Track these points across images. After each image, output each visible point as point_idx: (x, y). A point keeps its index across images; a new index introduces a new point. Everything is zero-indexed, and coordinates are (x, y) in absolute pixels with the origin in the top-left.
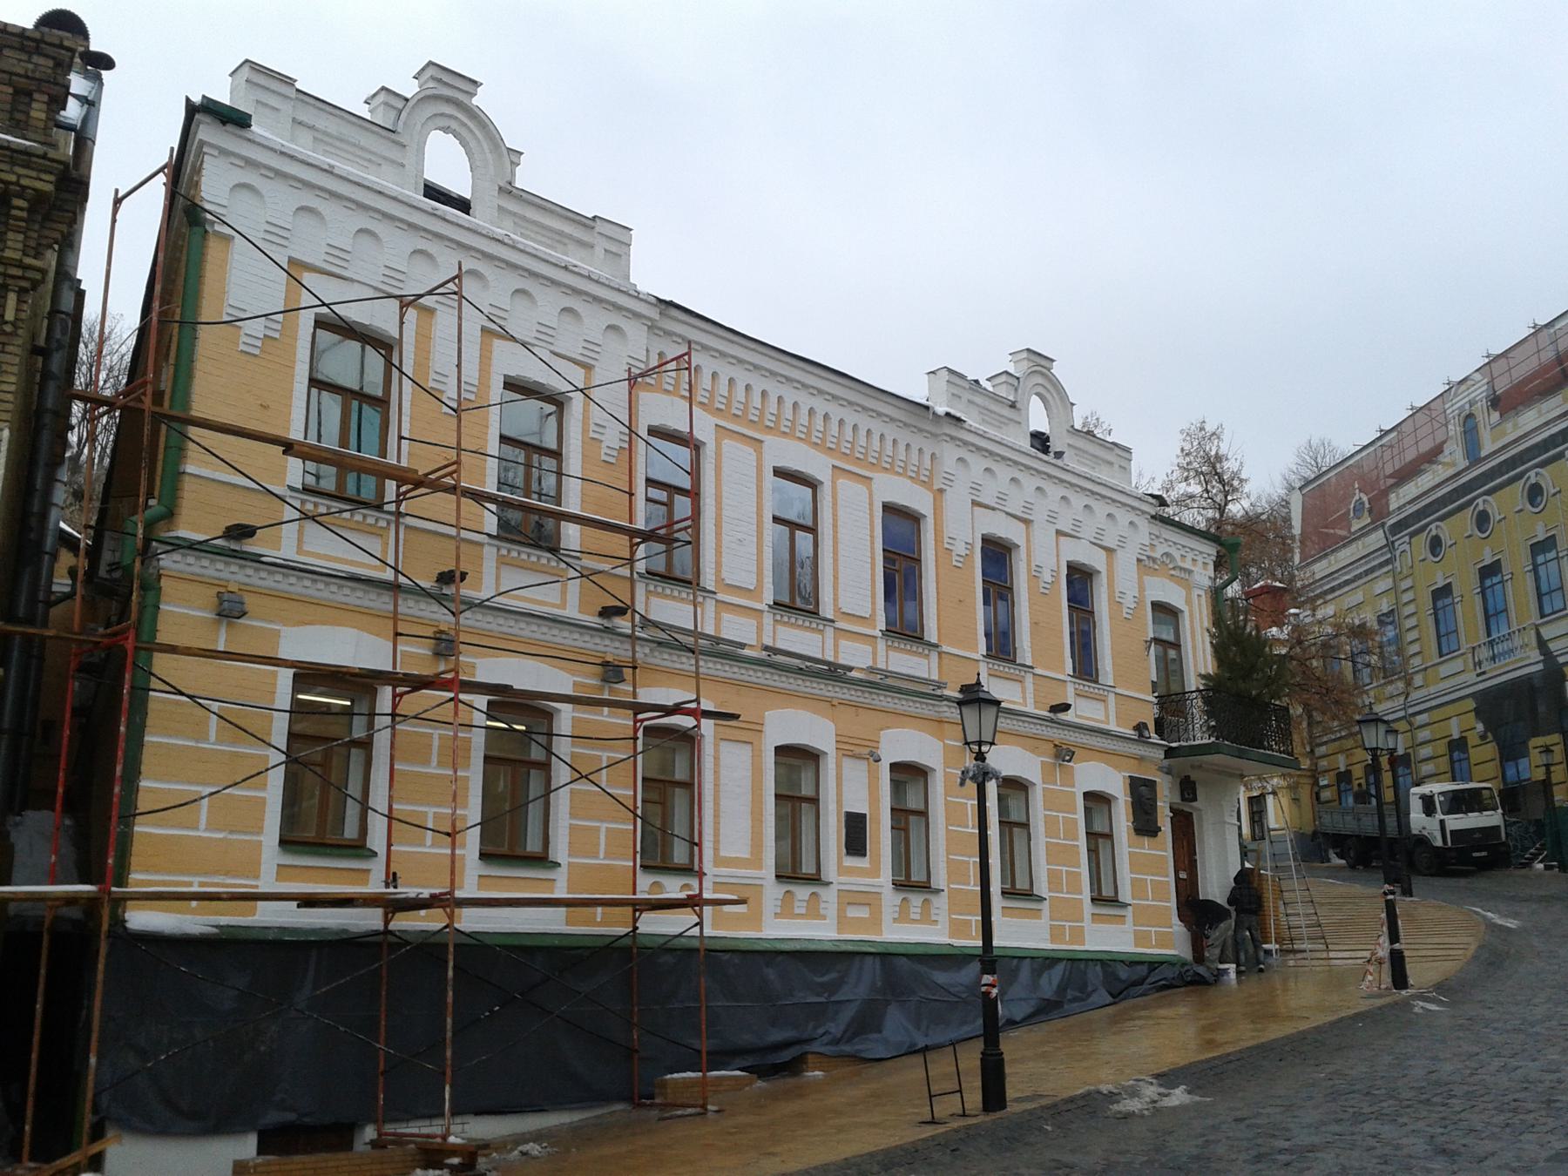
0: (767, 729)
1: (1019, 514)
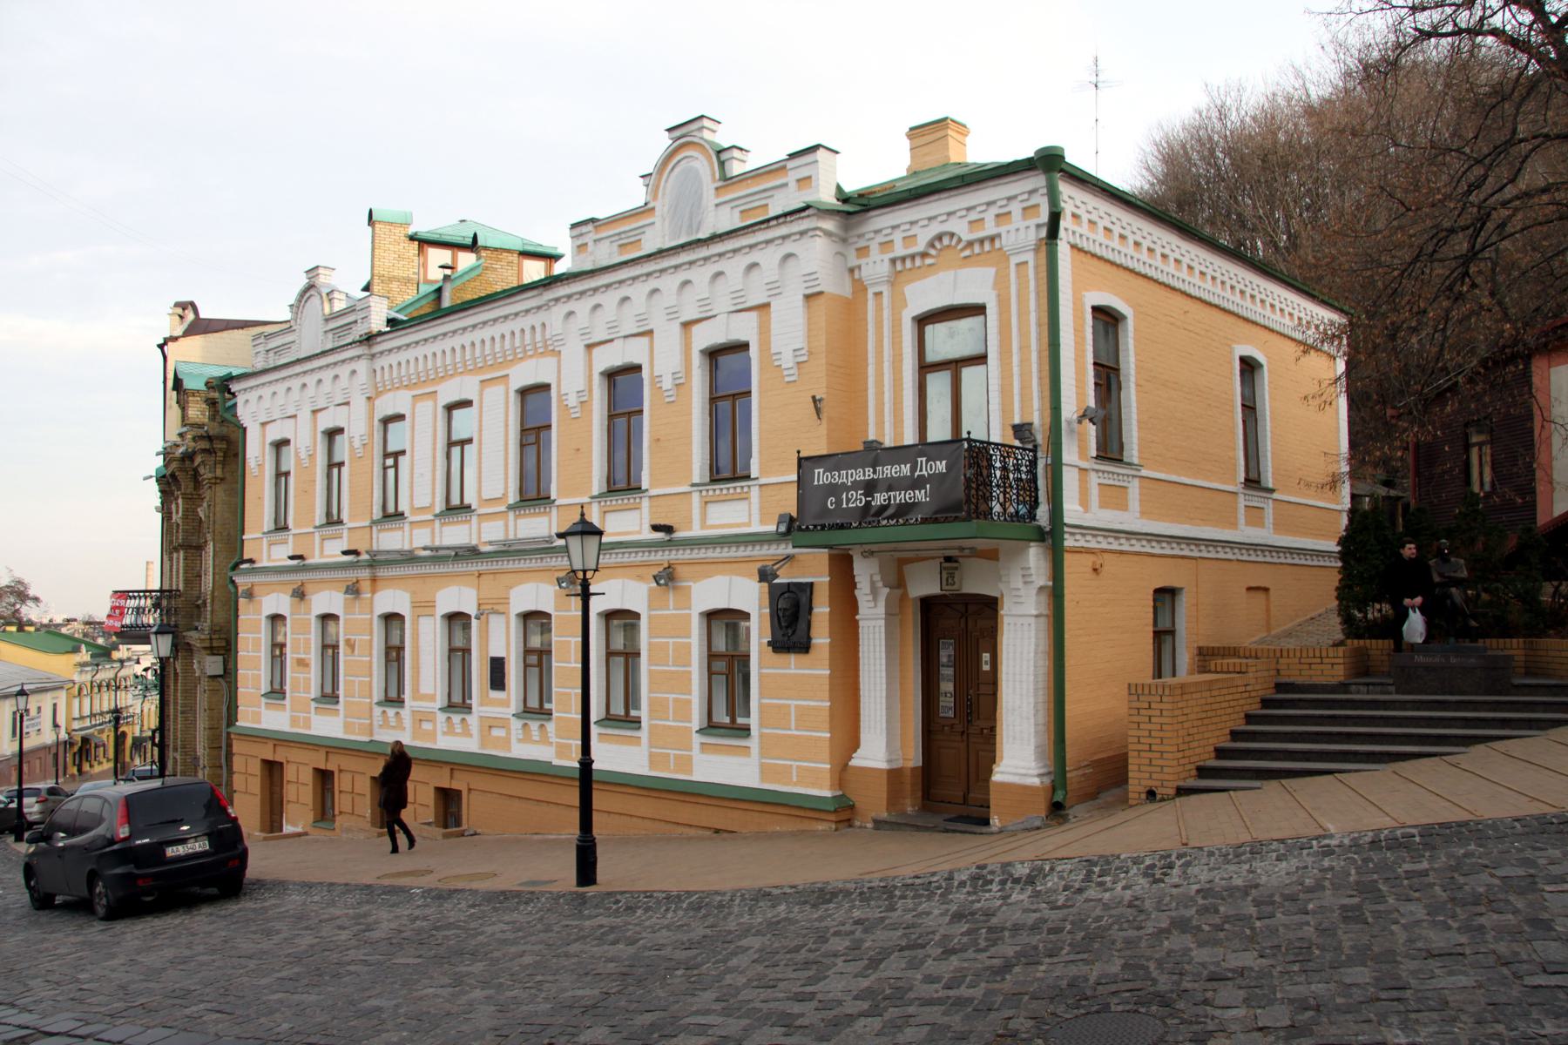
0: (438, 604)
1: (636, 331)
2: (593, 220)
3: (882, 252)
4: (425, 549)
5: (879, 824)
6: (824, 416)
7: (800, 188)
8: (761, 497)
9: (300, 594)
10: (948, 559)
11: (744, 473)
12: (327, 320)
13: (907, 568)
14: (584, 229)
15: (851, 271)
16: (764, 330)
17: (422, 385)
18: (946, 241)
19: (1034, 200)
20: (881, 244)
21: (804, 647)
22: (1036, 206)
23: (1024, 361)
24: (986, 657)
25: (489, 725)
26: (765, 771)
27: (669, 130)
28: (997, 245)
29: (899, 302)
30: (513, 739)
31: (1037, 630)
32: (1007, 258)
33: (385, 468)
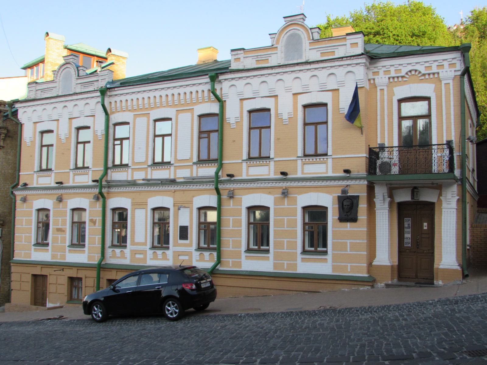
2: (243, 49)
3: (385, 74)
4: (143, 180)
5: (387, 286)
6: (364, 133)
7: (352, 47)
8: (333, 162)
9: (60, 200)
10: (415, 188)
11: (268, 156)
12: (77, 79)
13: (394, 191)
14: (239, 52)
15: (369, 80)
16: (336, 100)
17: (141, 111)
18: (413, 73)
19: (454, 62)
20: (384, 71)
21: (354, 220)
22: (455, 64)
23: (448, 118)
24: (425, 224)
25: (177, 254)
26: (334, 268)
27: (284, 18)
28: (436, 76)
29: (391, 94)
30: (194, 260)
31: (457, 214)
32: (440, 81)
33: (114, 145)
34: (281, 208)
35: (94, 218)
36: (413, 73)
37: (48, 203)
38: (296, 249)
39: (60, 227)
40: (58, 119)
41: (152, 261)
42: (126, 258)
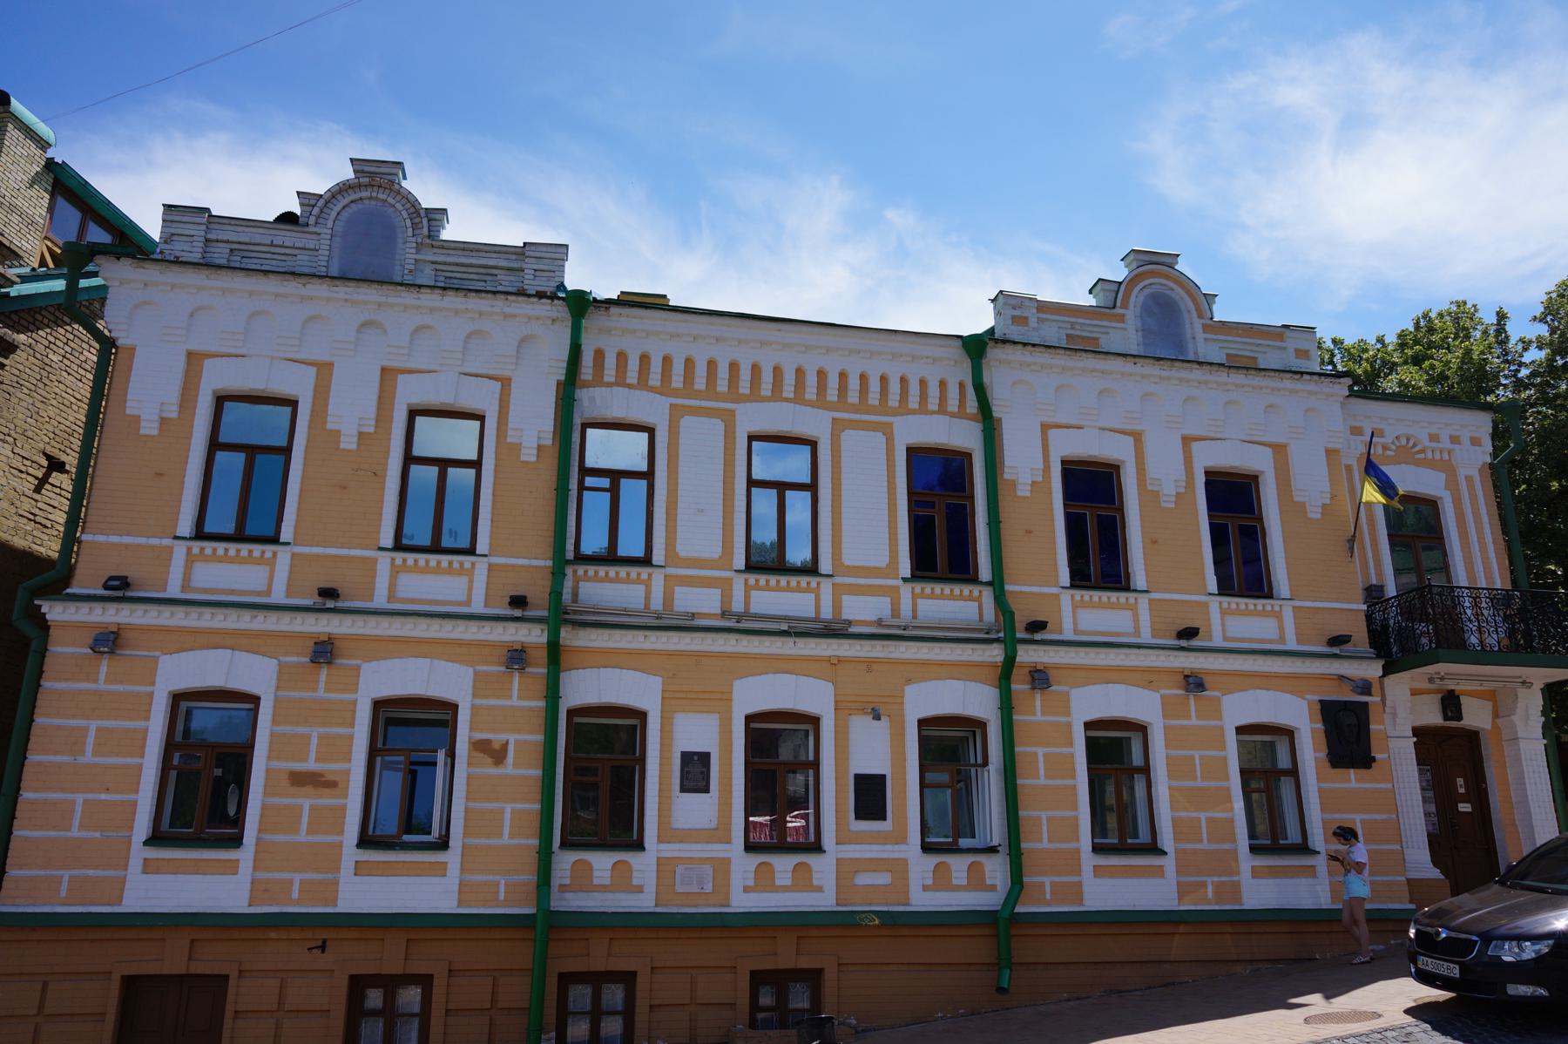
24: (1460, 781)
25: (845, 870)
33: (582, 488)
34: (1183, 727)
35: (497, 738)
36: (1404, 442)
37: (251, 673)
38: (1234, 840)
39: (311, 765)
40: (326, 358)
41: (753, 895)
42: (639, 889)
